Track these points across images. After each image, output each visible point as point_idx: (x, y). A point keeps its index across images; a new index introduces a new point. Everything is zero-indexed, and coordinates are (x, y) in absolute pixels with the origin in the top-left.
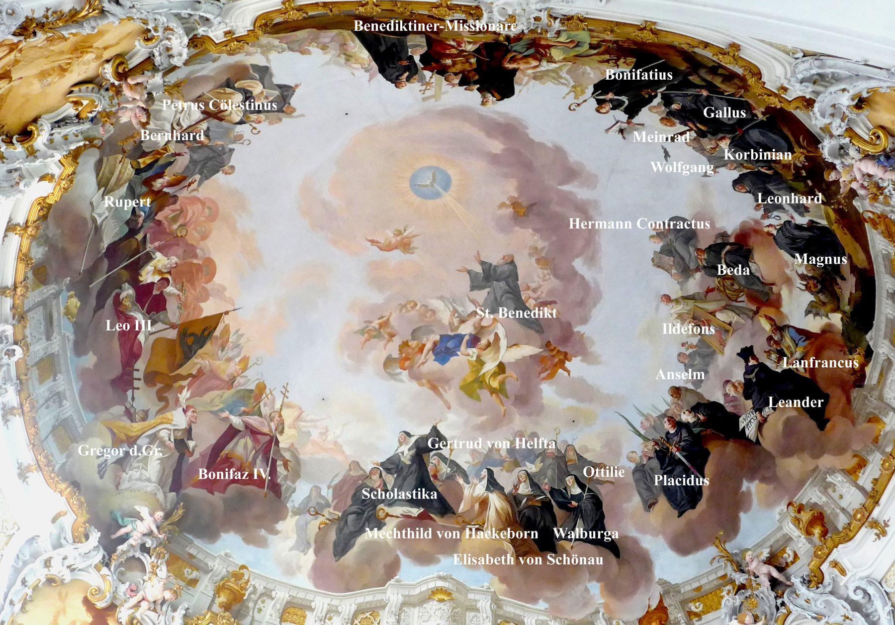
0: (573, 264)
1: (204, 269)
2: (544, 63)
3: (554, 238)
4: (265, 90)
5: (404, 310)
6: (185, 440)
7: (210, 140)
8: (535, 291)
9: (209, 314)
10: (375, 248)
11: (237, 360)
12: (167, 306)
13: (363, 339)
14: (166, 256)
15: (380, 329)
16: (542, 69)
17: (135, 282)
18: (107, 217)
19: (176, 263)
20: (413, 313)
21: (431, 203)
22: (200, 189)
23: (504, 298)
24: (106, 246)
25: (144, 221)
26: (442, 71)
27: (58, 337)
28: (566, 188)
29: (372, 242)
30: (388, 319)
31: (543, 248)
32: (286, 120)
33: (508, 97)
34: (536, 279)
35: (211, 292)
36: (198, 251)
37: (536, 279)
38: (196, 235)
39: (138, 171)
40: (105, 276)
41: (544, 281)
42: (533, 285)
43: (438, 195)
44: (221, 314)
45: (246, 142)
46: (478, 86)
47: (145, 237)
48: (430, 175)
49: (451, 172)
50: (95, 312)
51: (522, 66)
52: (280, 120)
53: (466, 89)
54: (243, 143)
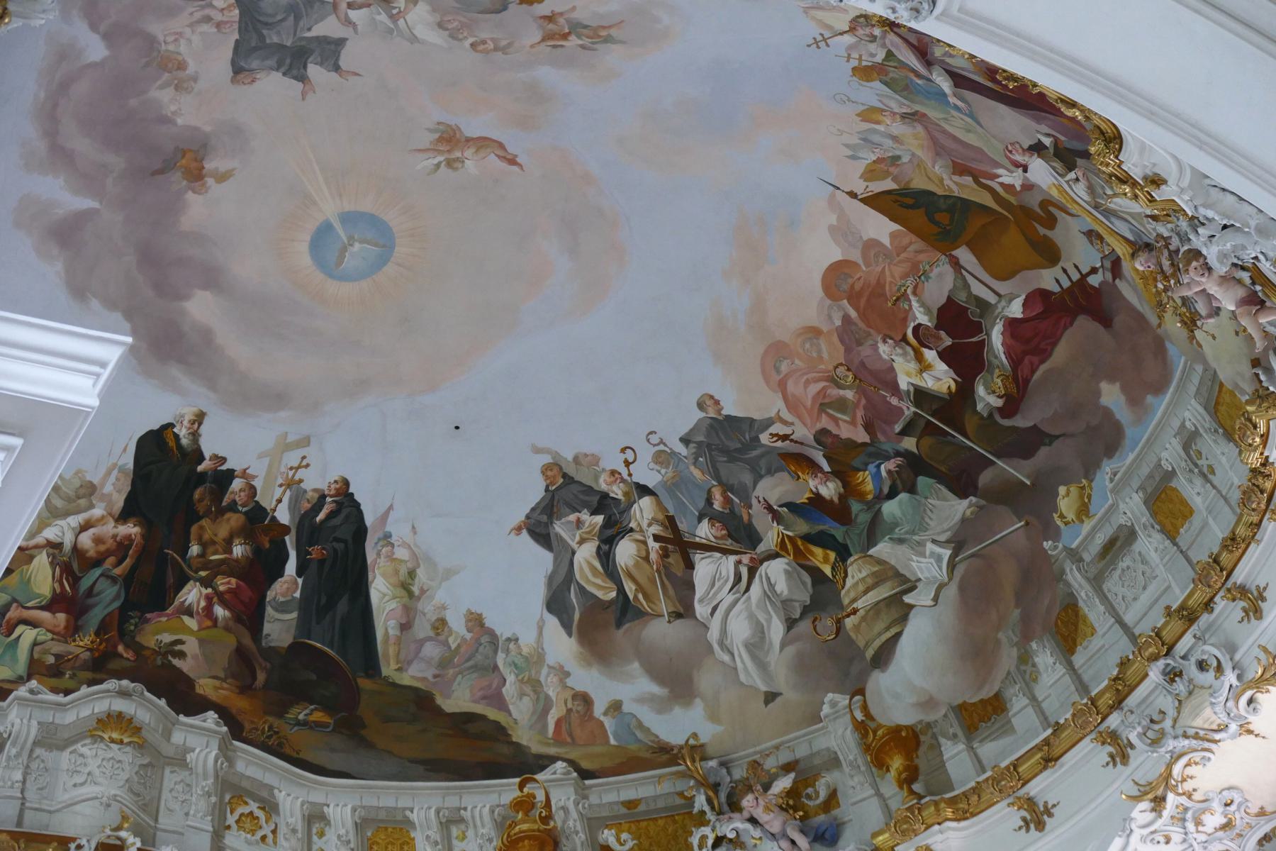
0: (106, 53)
1: (845, 287)
2: (68, 541)
3: (133, 102)
4: (574, 545)
5: (504, 43)
6: (1052, 151)
7: (709, 491)
8: (208, 19)
9: (884, 220)
10: (510, 150)
11: (881, 128)
12: (943, 300)
13: (613, 32)
14: (892, 369)
15: (569, 33)
16: (74, 521)
17: (964, 392)
18: (934, 541)
19: (885, 342)
20: (484, 36)
21: (366, 205)
22: (773, 414)
23: (279, 17)
24: (965, 503)
25: (888, 458)
26: (257, 516)
27: (1122, 506)
28: (86, 203)
29: (512, 161)
30: (543, 40)
31: (162, 87)
32: (569, 455)
33: (151, 433)
34: (196, 39)
35: (860, 245)
36: (838, 323)
37: (196, 39)
38: (824, 347)
39: (843, 554)
40: (999, 463)
41: (180, 34)
42: (205, 28)
43: (347, 218)
44: (863, 200)
45: (654, 439)
46: (200, 468)
47: (905, 432)
48: (350, 262)
49: (303, 257)
50: (1053, 438)
51: (110, 529)
52: (576, 459)
53: (223, 460)
54: (662, 442)
